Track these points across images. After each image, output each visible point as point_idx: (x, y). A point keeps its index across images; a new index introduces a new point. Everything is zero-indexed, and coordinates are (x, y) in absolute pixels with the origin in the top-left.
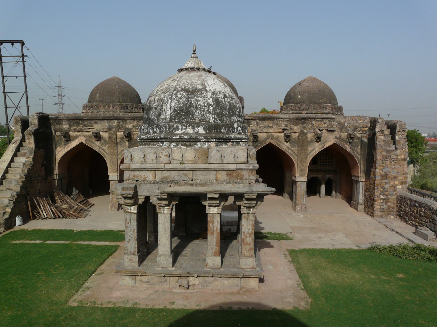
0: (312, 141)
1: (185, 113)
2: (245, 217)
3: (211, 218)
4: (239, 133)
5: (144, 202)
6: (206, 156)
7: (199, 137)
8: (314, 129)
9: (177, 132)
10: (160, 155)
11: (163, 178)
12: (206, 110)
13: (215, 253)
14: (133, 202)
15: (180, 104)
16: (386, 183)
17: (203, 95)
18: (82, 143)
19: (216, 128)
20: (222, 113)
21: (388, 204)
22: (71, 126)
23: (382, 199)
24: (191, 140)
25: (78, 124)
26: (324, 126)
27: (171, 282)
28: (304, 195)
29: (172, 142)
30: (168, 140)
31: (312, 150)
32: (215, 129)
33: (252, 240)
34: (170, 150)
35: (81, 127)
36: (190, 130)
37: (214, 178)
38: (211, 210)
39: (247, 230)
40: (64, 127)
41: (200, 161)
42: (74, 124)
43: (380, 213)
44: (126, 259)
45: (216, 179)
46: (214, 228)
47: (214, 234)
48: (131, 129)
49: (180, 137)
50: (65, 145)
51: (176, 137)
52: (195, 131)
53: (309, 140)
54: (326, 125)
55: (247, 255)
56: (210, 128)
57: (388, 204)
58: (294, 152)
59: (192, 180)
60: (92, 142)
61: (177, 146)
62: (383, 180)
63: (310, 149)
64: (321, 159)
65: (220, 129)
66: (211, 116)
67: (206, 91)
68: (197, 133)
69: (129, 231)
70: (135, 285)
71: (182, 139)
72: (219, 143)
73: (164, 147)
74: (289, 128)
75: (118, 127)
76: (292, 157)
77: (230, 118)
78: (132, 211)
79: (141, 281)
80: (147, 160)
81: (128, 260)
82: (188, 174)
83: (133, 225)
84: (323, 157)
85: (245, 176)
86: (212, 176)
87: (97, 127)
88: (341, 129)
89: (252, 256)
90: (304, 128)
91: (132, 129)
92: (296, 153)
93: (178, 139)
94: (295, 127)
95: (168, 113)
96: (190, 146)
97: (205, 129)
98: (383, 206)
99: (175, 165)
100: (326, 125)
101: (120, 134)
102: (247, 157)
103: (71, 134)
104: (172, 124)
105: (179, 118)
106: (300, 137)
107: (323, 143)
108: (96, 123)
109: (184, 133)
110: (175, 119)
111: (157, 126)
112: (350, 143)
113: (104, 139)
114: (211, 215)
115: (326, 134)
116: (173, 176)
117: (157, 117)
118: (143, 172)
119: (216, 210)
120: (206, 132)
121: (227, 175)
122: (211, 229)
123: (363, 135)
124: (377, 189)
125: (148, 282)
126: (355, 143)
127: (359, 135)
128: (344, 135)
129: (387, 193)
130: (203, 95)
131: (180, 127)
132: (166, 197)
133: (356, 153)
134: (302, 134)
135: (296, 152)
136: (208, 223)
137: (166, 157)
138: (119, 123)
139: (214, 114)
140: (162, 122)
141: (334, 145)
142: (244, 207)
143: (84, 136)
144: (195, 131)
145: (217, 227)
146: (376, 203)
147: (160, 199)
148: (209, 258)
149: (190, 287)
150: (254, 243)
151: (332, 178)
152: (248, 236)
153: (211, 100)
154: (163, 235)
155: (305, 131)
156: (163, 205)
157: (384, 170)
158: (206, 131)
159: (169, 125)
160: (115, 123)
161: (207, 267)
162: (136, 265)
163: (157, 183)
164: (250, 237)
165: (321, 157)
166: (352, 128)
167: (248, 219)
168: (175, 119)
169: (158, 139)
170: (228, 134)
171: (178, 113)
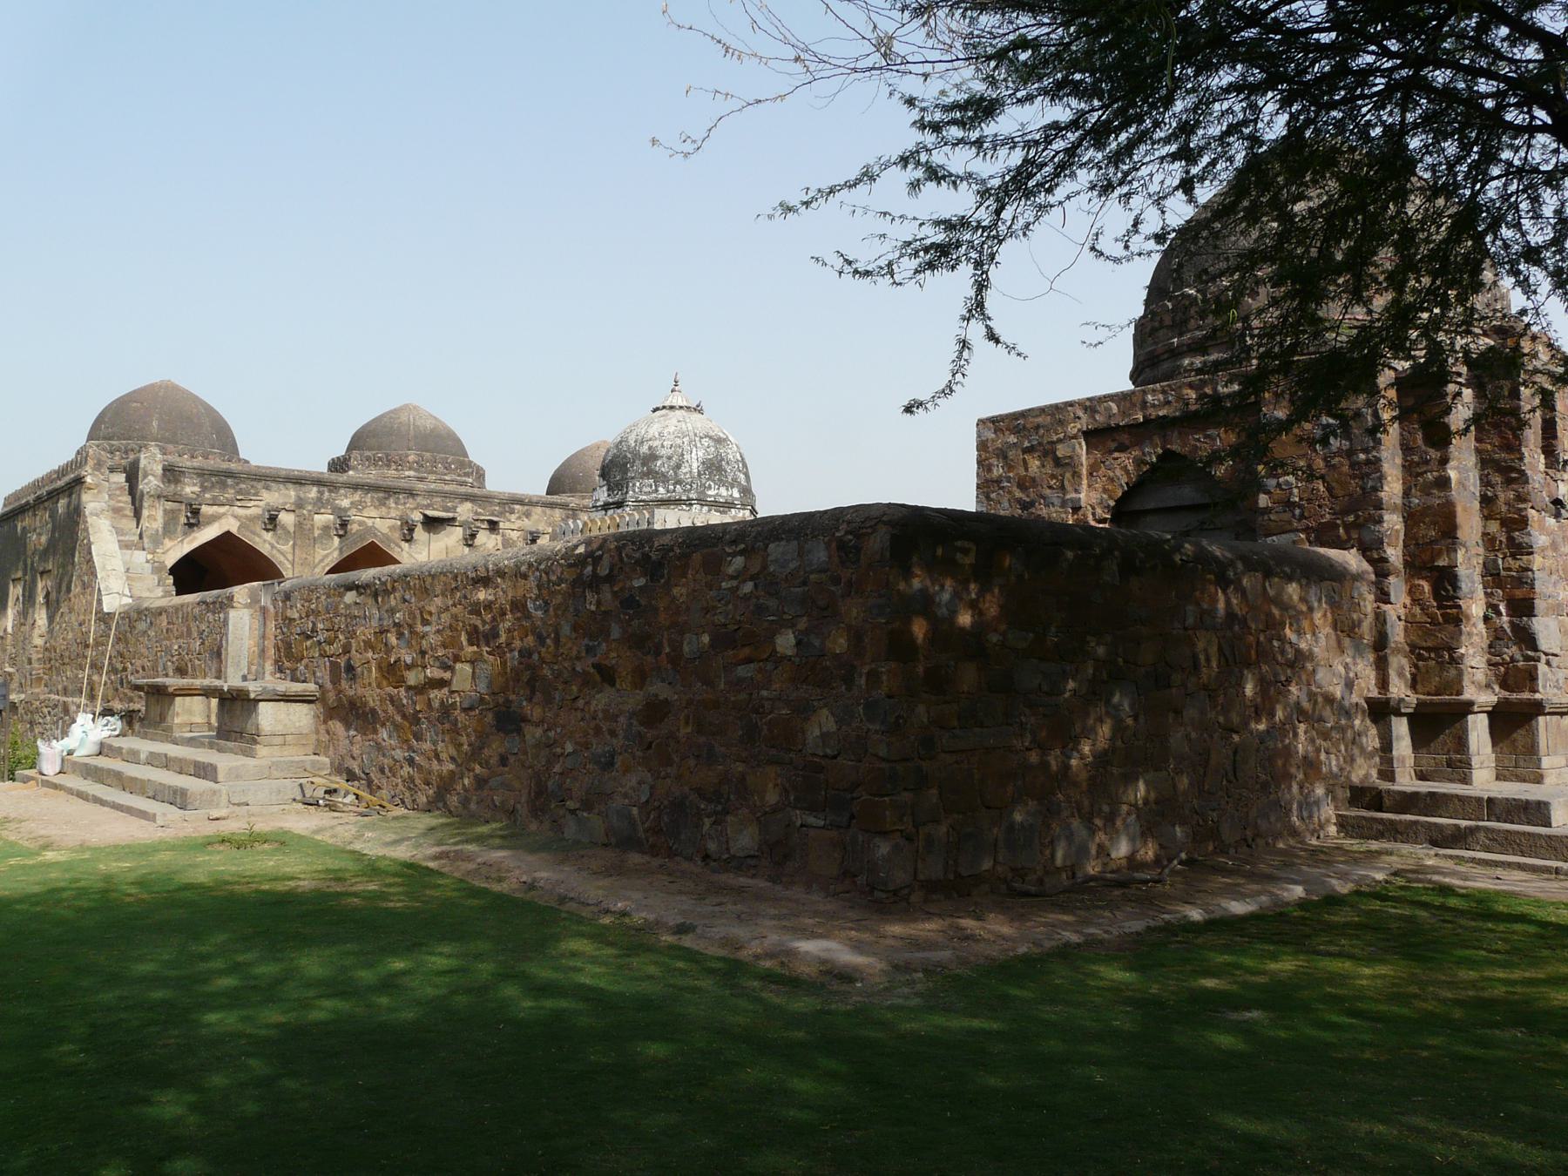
18: (228, 534)
22: (204, 489)
25: (224, 486)
35: (230, 494)
36: (723, 491)
40: (188, 490)
42: (213, 486)
48: (346, 510)
50: (185, 534)
60: (254, 533)
75: (319, 504)
87: (272, 497)
95: (695, 465)
101: (324, 518)
103: (204, 509)
111: (679, 482)
113: (284, 528)
138: (322, 493)
160: (313, 492)
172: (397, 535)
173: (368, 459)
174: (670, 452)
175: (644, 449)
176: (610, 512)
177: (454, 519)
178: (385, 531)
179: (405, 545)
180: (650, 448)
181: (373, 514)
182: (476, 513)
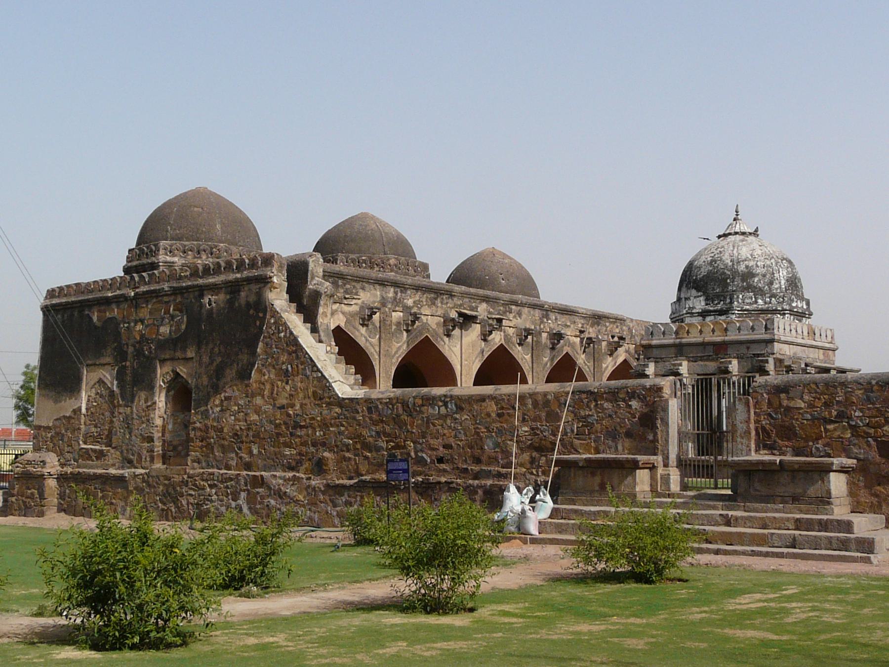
63: (604, 366)
91: (413, 307)
95: (783, 282)
108: (363, 289)
111: (773, 296)
143: (343, 313)
160: (391, 293)
172: (441, 331)
173: (353, 261)
174: (764, 271)
175: (742, 268)
176: (708, 319)
177: (475, 317)
178: (434, 327)
179: (446, 339)
180: (747, 267)
182: (490, 313)
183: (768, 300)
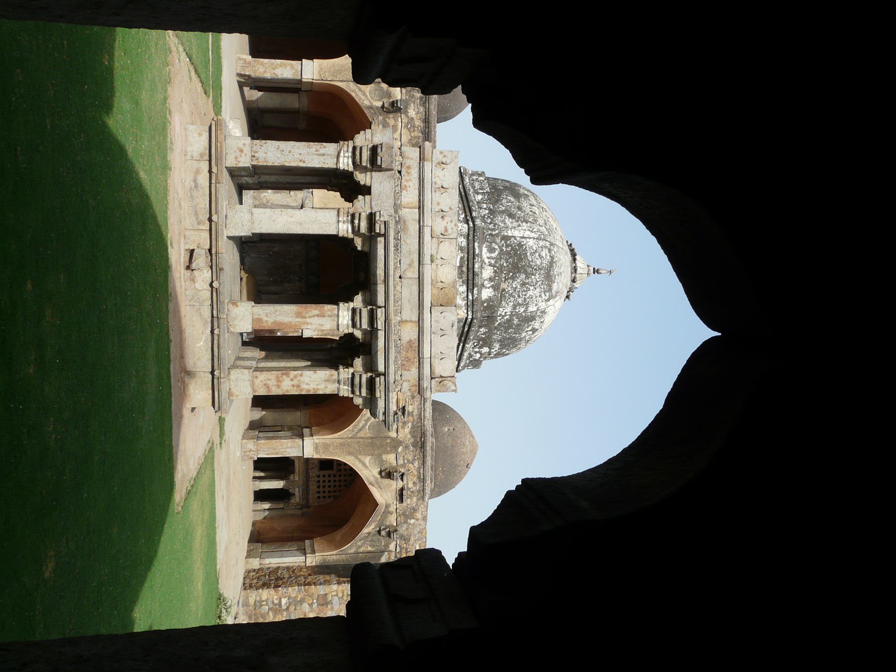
0: (382, 462)
1: (517, 264)
2: (332, 375)
3: (329, 313)
4: (470, 356)
5: (358, 183)
6: (445, 302)
7: (476, 289)
8: (403, 466)
9: (485, 250)
10: (447, 219)
11: (404, 221)
12: (520, 300)
13: (260, 320)
14: (364, 164)
15: (532, 254)
16: (311, 605)
17: (543, 295)
19: (490, 318)
20: (510, 327)
21: (271, 613)
23: (280, 601)
24: (471, 276)
26: (410, 483)
27: (197, 233)
28: (277, 454)
29: (468, 239)
30: (471, 233)
31: (364, 464)
32: (488, 317)
33: (287, 391)
34: (454, 236)
37: (404, 318)
38: (346, 313)
39: (307, 380)
41: (435, 291)
43: (252, 601)
44: (243, 142)
45: (402, 322)
46: (310, 317)
47: (297, 317)
48: (406, 113)
49: (478, 255)
51: (476, 247)
52: (486, 282)
53: (384, 457)
54: (411, 485)
55: (257, 382)
56: (491, 307)
57: (271, 613)
58: (360, 430)
59: (400, 277)
61: (461, 249)
62: (317, 599)
63: (367, 460)
64: (329, 476)
65: (485, 326)
66: (509, 309)
67: (548, 300)
68: (483, 285)
69: (301, 151)
70: (188, 157)
71: (474, 258)
72: (462, 324)
73: (460, 225)
74: (406, 419)
76: (350, 427)
77: (500, 341)
78: (341, 160)
79: (198, 172)
80: (438, 194)
81: (241, 146)
82: (411, 270)
83: (312, 159)
84: (335, 481)
85: (408, 373)
86: (409, 313)
88: (404, 514)
89: (254, 391)
90: (406, 447)
91: (407, 117)
92: (359, 435)
93: (474, 252)
94: (407, 430)
95: (516, 233)
96: (461, 272)
97: (490, 300)
98: (267, 604)
99: (429, 245)
100: (411, 485)
102: (441, 377)
104: (498, 241)
105: (508, 253)
106: (389, 441)
107: (378, 484)
109: (483, 261)
110: (507, 246)
111: (492, 212)
112: (379, 532)
114: (336, 312)
115: (394, 487)
116: (408, 241)
117: (506, 210)
118: (417, 186)
119: (345, 322)
120: (484, 302)
121: (410, 341)
122: (307, 313)
123: (393, 554)
124: (299, 591)
125: (196, 186)
126: (379, 540)
127: (392, 547)
128: (392, 520)
129: (292, 608)
130: (543, 295)
131: (493, 255)
132: (378, 231)
133: (359, 543)
134: (396, 444)
135: (361, 434)
136: (328, 308)
137: (443, 230)
139: (511, 315)
140: (498, 219)
141: (376, 504)
142: (353, 374)
144: (486, 282)
145: (311, 324)
146: (272, 591)
147: (371, 218)
148: (250, 308)
149: (188, 273)
150: (281, 393)
151: (292, 501)
152: (295, 382)
153: (535, 309)
154: (292, 219)
155: (400, 449)
156: (356, 222)
157: (336, 598)
158: (486, 301)
159: (497, 235)
161: (230, 305)
162: (230, 162)
163: (396, 212)
164: (293, 386)
165: (335, 476)
166: (405, 533)
167: (327, 381)
168: (507, 246)
169: (471, 214)
170: (474, 339)
171: (516, 251)
181: (404, 139)
183: (485, 206)
